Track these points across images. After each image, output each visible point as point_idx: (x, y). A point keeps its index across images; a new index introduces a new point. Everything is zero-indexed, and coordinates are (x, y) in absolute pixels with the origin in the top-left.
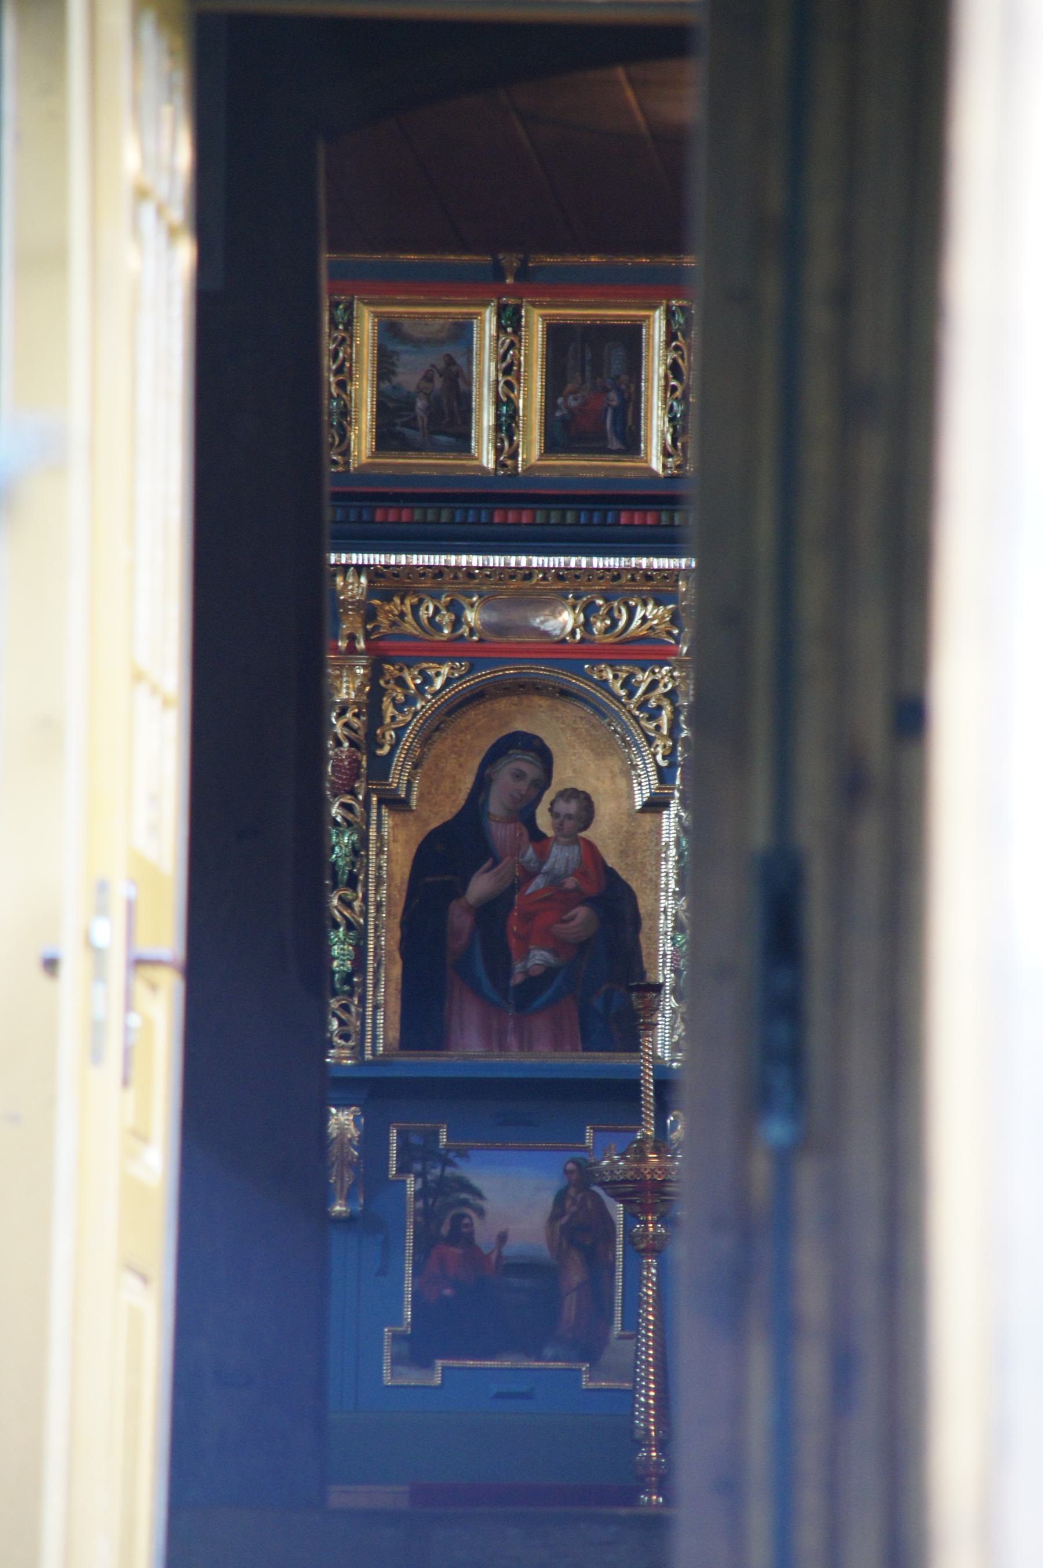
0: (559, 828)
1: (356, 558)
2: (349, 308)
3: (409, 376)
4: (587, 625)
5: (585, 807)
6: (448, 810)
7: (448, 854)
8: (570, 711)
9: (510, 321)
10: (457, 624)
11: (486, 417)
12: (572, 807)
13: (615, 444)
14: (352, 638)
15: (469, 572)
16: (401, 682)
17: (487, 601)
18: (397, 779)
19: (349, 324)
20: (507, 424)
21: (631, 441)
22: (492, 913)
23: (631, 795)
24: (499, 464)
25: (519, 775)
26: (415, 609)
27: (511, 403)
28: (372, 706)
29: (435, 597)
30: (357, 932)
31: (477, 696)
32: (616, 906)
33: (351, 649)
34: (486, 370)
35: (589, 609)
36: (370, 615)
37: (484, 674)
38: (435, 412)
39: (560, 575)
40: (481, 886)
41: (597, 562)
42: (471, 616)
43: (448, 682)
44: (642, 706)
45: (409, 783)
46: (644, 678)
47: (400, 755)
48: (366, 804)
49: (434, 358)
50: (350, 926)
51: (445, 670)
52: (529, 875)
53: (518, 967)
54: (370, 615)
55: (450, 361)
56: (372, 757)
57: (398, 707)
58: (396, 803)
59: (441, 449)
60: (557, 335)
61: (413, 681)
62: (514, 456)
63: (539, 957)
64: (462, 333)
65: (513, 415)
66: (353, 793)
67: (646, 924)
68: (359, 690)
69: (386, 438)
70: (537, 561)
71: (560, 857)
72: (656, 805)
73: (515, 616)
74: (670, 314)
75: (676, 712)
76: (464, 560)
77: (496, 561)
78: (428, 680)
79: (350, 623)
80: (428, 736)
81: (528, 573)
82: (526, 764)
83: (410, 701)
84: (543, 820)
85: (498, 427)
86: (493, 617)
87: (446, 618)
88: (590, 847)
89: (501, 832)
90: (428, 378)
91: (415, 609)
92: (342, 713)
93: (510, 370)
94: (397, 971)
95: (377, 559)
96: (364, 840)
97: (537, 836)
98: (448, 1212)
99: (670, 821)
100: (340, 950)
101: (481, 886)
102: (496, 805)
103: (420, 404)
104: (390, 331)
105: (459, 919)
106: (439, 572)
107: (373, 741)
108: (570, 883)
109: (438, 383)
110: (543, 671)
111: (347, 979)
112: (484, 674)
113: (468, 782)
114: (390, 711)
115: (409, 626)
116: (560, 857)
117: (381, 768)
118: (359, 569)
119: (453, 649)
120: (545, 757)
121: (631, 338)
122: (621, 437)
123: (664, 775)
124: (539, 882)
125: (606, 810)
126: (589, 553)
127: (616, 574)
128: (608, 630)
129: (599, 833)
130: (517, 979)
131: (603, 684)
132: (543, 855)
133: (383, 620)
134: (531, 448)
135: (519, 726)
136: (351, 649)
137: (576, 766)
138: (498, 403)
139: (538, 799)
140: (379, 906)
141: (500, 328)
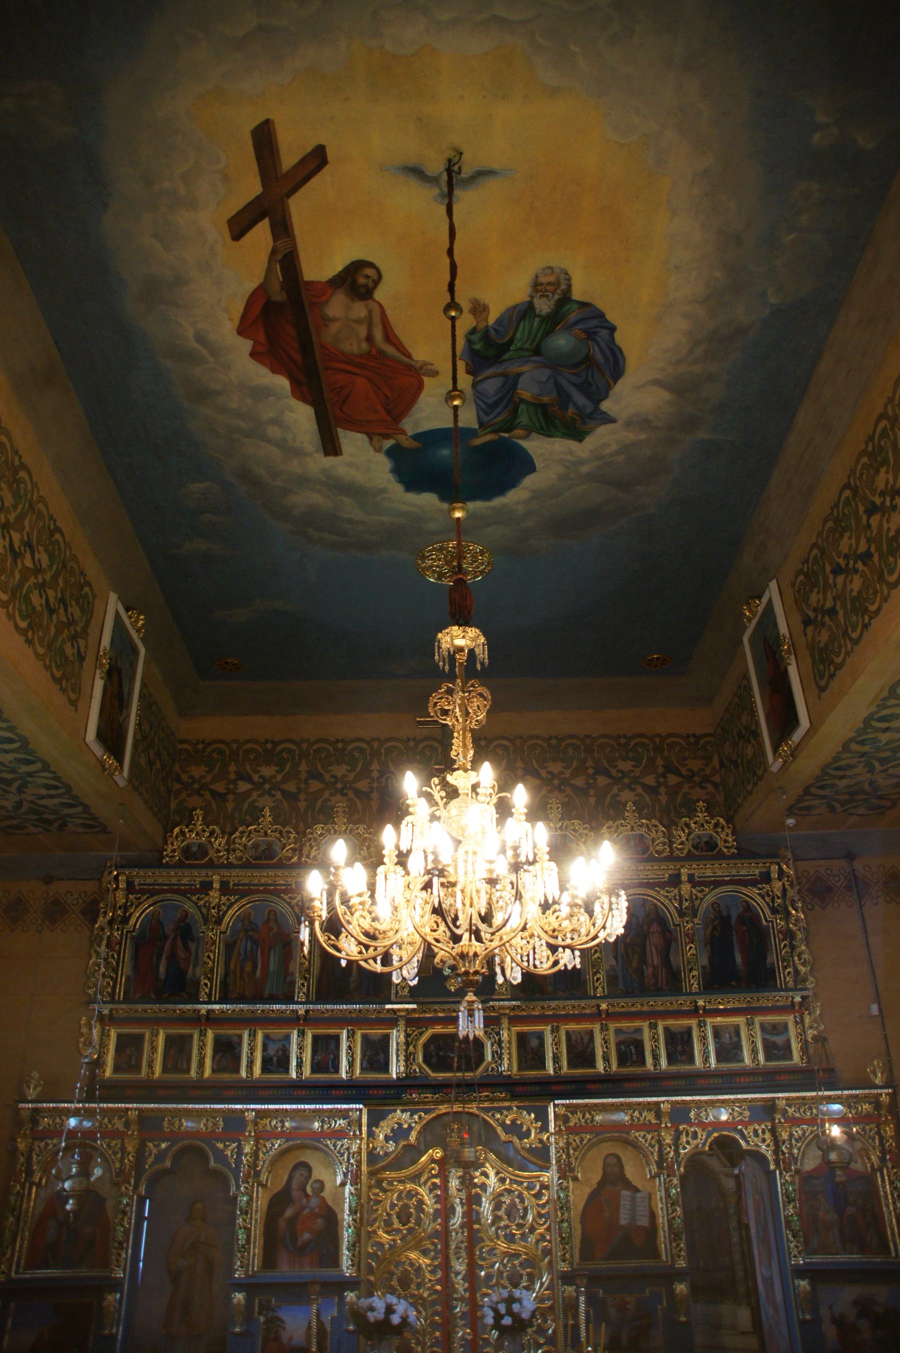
0: (313, 1192)
1: (252, 1106)
2: (255, 1030)
3: (271, 1051)
4: (322, 1127)
5: (321, 1185)
6: (280, 1186)
7: (279, 1201)
8: (318, 1154)
9: (302, 1034)
10: (283, 1126)
11: (294, 1063)
12: (317, 1186)
13: (332, 1070)
14: (250, 1132)
15: (286, 1110)
16: (265, 1146)
17: (292, 1119)
18: (263, 1177)
19: (254, 1036)
20: (300, 1065)
21: (337, 1069)
22: (292, 1221)
23: (336, 1181)
24: (297, 1077)
25: (302, 1175)
26: (270, 1122)
27: (301, 1058)
28: (255, 1154)
29: (276, 1118)
30: (248, 1231)
31: (288, 1150)
32: (331, 1218)
33: (250, 1135)
34: (294, 1048)
35: (323, 1121)
36: (256, 1123)
37: (291, 1143)
38: (279, 1061)
39: (314, 1111)
40: (289, 1212)
41: (325, 1106)
42: (287, 1124)
43: (279, 1145)
44: (339, 1152)
45: (267, 1179)
46: (339, 1143)
47: (264, 1169)
48: (253, 1186)
49: (278, 1046)
50: (245, 1228)
51: (279, 1142)
52: (304, 1208)
53: (300, 1240)
54: (256, 1123)
55: (284, 1046)
56: (255, 1171)
57: (264, 1154)
58: (264, 1186)
59: (280, 1073)
60: (315, 1038)
61: (269, 1145)
62: (302, 1074)
63: (307, 1236)
64: (288, 1038)
65: (302, 1061)
66: (248, 1183)
67: (340, 1224)
68: (251, 1149)
69: (265, 1069)
70: (307, 1106)
71: (314, 1202)
72: (343, 1184)
73: (305, 1124)
74: (348, 1031)
75: (349, 1154)
76: (285, 1106)
77: (294, 1106)
78: (273, 1145)
79: (250, 1127)
80: (274, 1161)
81: (304, 1110)
82: (303, 1171)
83: (268, 1152)
84: (309, 1190)
85: (297, 1066)
86: (294, 1124)
87: (280, 1125)
88: (323, 1198)
89: (296, 1194)
90: (277, 1051)
91: (270, 1122)
92: (246, 1155)
93: (301, 1048)
94: (262, 1242)
95: (259, 1106)
96: (251, 1199)
97: (307, 1195)
98: (275, 1323)
99: (348, 1188)
100: (241, 1236)
101: (289, 1212)
102: (294, 1185)
103: (275, 1059)
104: (267, 1037)
105: (282, 1224)
106: (277, 1110)
107: (256, 1165)
108: (317, 1210)
109: (280, 1052)
110: (309, 1142)
111: (243, 1246)
112: (291, 1143)
113: (286, 1178)
114: (261, 1155)
115: (268, 1128)
116: (314, 1202)
117: (257, 1174)
118: (252, 1110)
119: (282, 1135)
120: (309, 1169)
121: (337, 1039)
122: (333, 1068)
123: (345, 1175)
124: (307, 1211)
125: (328, 1186)
126: (322, 1104)
127: (331, 1110)
128: (329, 1128)
129: (326, 1194)
130: (300, 1244)
131: (327, 1146)
132: (308, 1200)
133: (260, 1126)
134: (307, 1071)
135: (302, 1159)
136: (250, 1135)
137: (319, 1172)
138: (297, 1058)
139: (307, 1183)
140: (256, 1220)
141: (299, 1036)
